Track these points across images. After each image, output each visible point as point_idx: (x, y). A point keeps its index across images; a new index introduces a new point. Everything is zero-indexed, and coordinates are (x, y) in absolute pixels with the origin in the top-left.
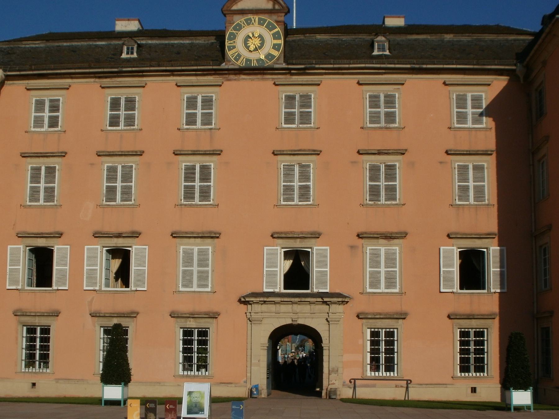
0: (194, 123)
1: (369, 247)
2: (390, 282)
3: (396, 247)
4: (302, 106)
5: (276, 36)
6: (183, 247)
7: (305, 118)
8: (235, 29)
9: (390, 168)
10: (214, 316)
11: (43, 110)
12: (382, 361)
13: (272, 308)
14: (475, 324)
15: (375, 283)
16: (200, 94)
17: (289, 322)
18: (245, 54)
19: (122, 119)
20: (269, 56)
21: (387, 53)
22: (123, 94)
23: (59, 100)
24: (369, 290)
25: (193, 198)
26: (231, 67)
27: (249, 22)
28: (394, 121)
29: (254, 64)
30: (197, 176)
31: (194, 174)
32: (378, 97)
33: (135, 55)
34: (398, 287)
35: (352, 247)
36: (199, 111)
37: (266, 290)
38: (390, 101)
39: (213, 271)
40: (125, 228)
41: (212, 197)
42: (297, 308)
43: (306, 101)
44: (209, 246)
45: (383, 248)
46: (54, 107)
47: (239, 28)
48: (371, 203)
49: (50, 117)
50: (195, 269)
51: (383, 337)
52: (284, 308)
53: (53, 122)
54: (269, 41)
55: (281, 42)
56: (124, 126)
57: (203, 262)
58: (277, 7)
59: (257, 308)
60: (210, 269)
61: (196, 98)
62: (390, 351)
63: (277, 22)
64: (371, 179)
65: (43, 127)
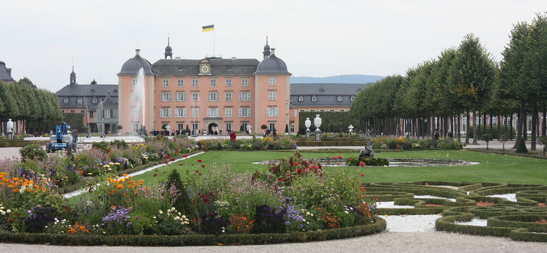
0: (194, 85)
2: (230, 115)
5: (209, 68)
7: (215, 85)
14: (245, 123)
18: (204, 72)
20: (208, 72)
22: (180, 80)
27: (204, 65)
35: (223, 109)
36: (195, 83)
38: (230, 81)
40: (182, 106)
42: (213, 120)
43: (215, 81)
45: (229, 109)
46: (167, 82)
47: (202, 66)
51: (229, 125)
52: (211, 120)
53: (167, 85)
57: (196, 112)
59: (206, 120)
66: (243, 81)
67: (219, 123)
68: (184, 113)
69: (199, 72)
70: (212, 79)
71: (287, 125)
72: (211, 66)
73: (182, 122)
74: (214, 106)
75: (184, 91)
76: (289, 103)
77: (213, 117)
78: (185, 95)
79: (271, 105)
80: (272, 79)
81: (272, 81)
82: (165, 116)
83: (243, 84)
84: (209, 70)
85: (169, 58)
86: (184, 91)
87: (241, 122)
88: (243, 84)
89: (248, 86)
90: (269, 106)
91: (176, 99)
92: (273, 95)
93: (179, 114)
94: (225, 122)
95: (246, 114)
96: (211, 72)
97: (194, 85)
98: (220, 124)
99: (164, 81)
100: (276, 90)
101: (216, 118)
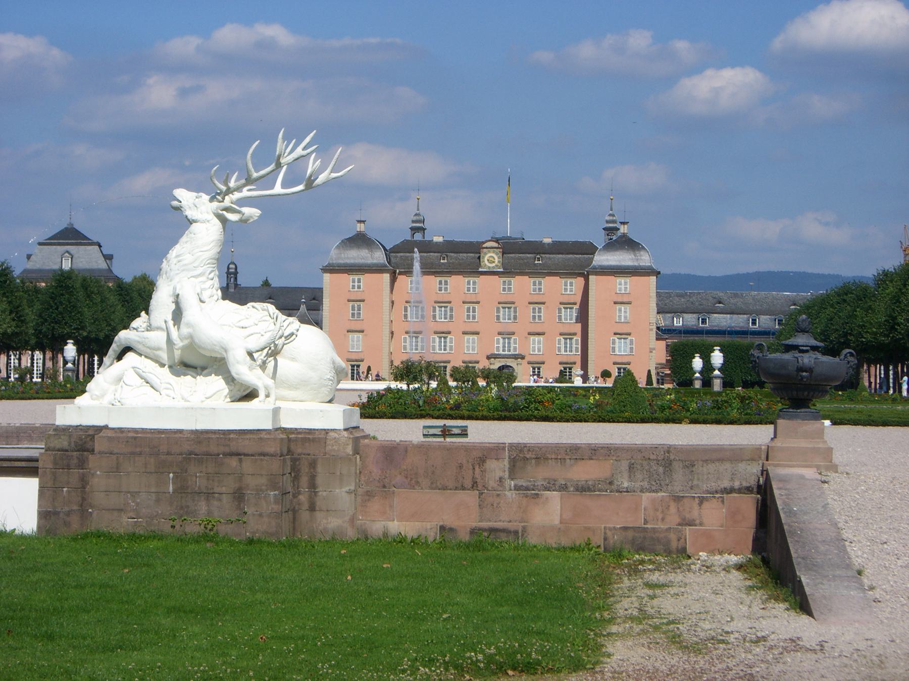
0: (470, 291)
1: (532, 338)
2: (539, 350)
3: (541, 338)
5: (499, 258)
6: (466, 337)
7: (510, 289)
13: (498, 360)
15: (534, 351)
16: (472, 280)
17: (504, 364)
19: (443, 289)
20: (497, 266)
21: (541, 262)
22: (443, 279)
26: (483, 270)
27: (489, 252)
30: (471, 311)
33: (446, 261)
36: (471, 286)
37: (496, 353)
38: (540, 283)
40: (445, 330)
42: (506, 359)
43: (510, 284)
44: (475, 337)
45: (537, 338)
47: (486, 254)
50: (471, 345)
54: (496, 260)
55: (501, 260)
57: (474, 343)
58: (500, 246)
59: (493, 359)
64: (533, 313)
66: (566, 285)
68: (448, 344)
69: (479, 265)
70: (505, 279)
71: (649, 371)
72: (503, 253)
73: (444, 362)
75: (450, 302)
76: (654, 327)
77: (506, 353)
78: (451, 310)
79: (620, 332)
80: (623, 281)
81: (623, 284)
83: (566, 290)
84: (499, 262)
85: (418, 237)
86: (450, 302)
87: (560, 363)
88: (566, 290)
89: (574, 294)
90: (615, 334)
91: (434, 317)
92: (624, 312)
93: (440, 346)
94: (529, 363)
95: (571, 347)
97: (469, 290)
98: (519, 366)
100: (629, 303)
101: (513, 355)
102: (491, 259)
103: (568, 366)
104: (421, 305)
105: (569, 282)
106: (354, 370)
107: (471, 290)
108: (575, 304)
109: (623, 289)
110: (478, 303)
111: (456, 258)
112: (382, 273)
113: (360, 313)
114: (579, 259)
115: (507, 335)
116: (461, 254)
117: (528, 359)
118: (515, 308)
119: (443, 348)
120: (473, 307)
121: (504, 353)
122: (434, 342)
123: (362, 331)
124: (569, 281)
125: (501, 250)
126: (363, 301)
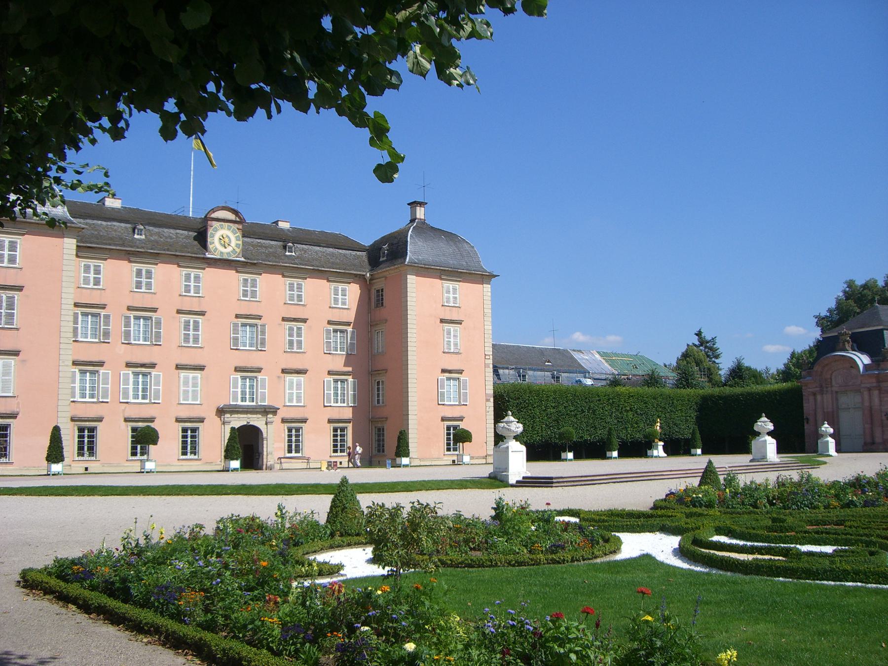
0: (189, 291)
1: (288, 377)
2: (299, 400)
3: (302, 378)
4: (252, 287)
5: (237, 239)
6: (183, 374)
7: (254, 294)
8: (213, 230)
9: (299, 329)
10: (201, 420)
11: (89, 273)
12: (293, 447)
13: (236, 416)
15: (291, 400)
16: (193, 272)
17: (245, 423)
19: (144, 284)
21: (293, 254)
22: (144, 267)
23: (100, 266)
24: (288, 404)
25: (189, 342)
28: (301, 301)
29: (225, 257)
30: (191, 327)
31: (189, 326)
32: (293, 284)
34: (303, 402)
35: (279, 377)
36: (192, 284)
37: (231, 403)
38: (300, 287)
39: (201, 390)
40: (146, 360)
41: (200, 342)
42: (249, 416)
43: (254, 283)
44: (198, 374)
45: (295, 378)
46: (97, 271)
47: (216, 230)
48: (289, 350)
49: (95, 278)
50: (190, 389)
53: (97, 282)
55: (240, 242)
56: (146, 289)
57: (195, 385)
58: (238, 219)
59: (228, 415)
60: (199, 389)
61: (190, 274)
62: (297, 441)
63: (238, 229)
65: (89, 284)
67: (266, 424)
70: (246, 276)
74: (249, 365)
75: (154, 310)
77: (248, 403)
79: (450, 368)
80: (451, 286)
82: (84, 396)
83: (336, 300)
88: (336, 300)
90: (443, 371)
91: (127, 334)
93: (136, 390)
94: (284, 421)
96: (244, 253)
97: (188, 290)
99: (87, 269)
102: (227, 240)
103: (88, 424)
104: (103, 312)
105: (340, 287)
106: (83, 437)
107: (192, 291)
108: (348, 324)
109: (452, 300)
110: (202, 313)
111: (158, 234)
112: (62, 236)
113: (12, 315)
114: (345, 255)
115: (247, 371)
116: (166, 230)
117: (282, 414)
118: (263, 326)
119: (140, 393)
120: (195, 322)
121: (243, 403)
122: (126, 382)
123: (16, 353)
124: (341, 286)
125: (240, 227)
126: (20, 289)
